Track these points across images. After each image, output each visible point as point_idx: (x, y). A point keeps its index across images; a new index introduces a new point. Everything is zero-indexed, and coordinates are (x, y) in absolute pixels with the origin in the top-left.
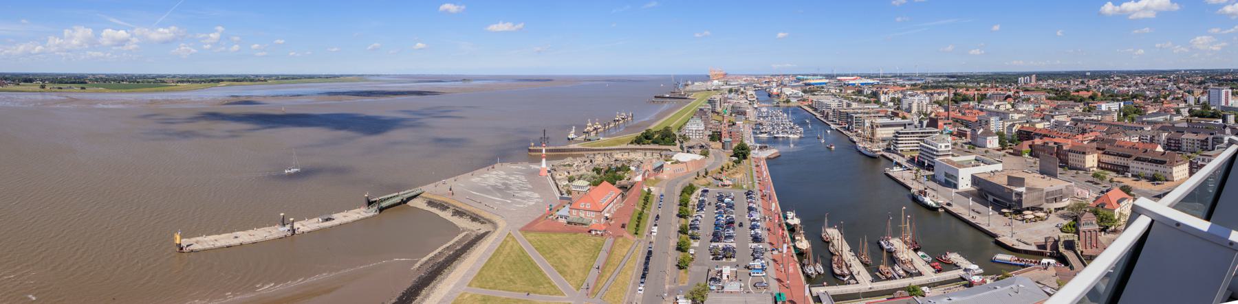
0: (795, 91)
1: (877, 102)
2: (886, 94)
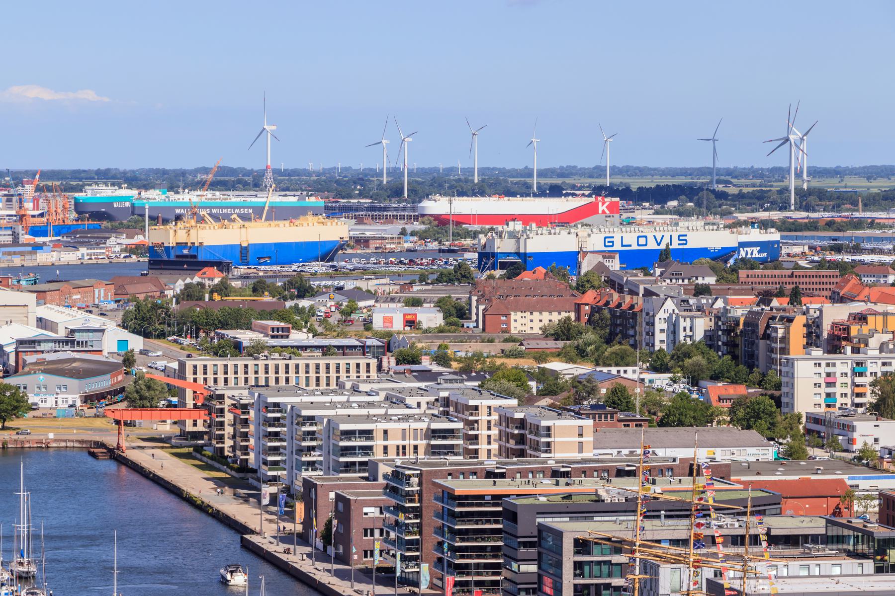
2: (834, 346)
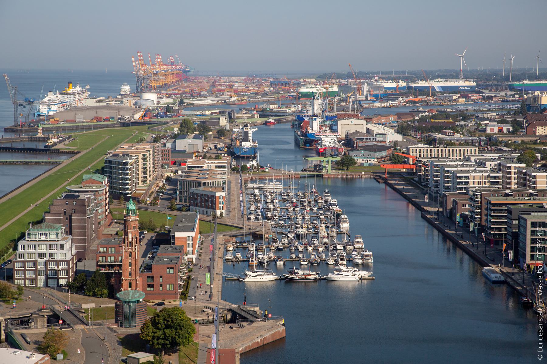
0: (376, 129)
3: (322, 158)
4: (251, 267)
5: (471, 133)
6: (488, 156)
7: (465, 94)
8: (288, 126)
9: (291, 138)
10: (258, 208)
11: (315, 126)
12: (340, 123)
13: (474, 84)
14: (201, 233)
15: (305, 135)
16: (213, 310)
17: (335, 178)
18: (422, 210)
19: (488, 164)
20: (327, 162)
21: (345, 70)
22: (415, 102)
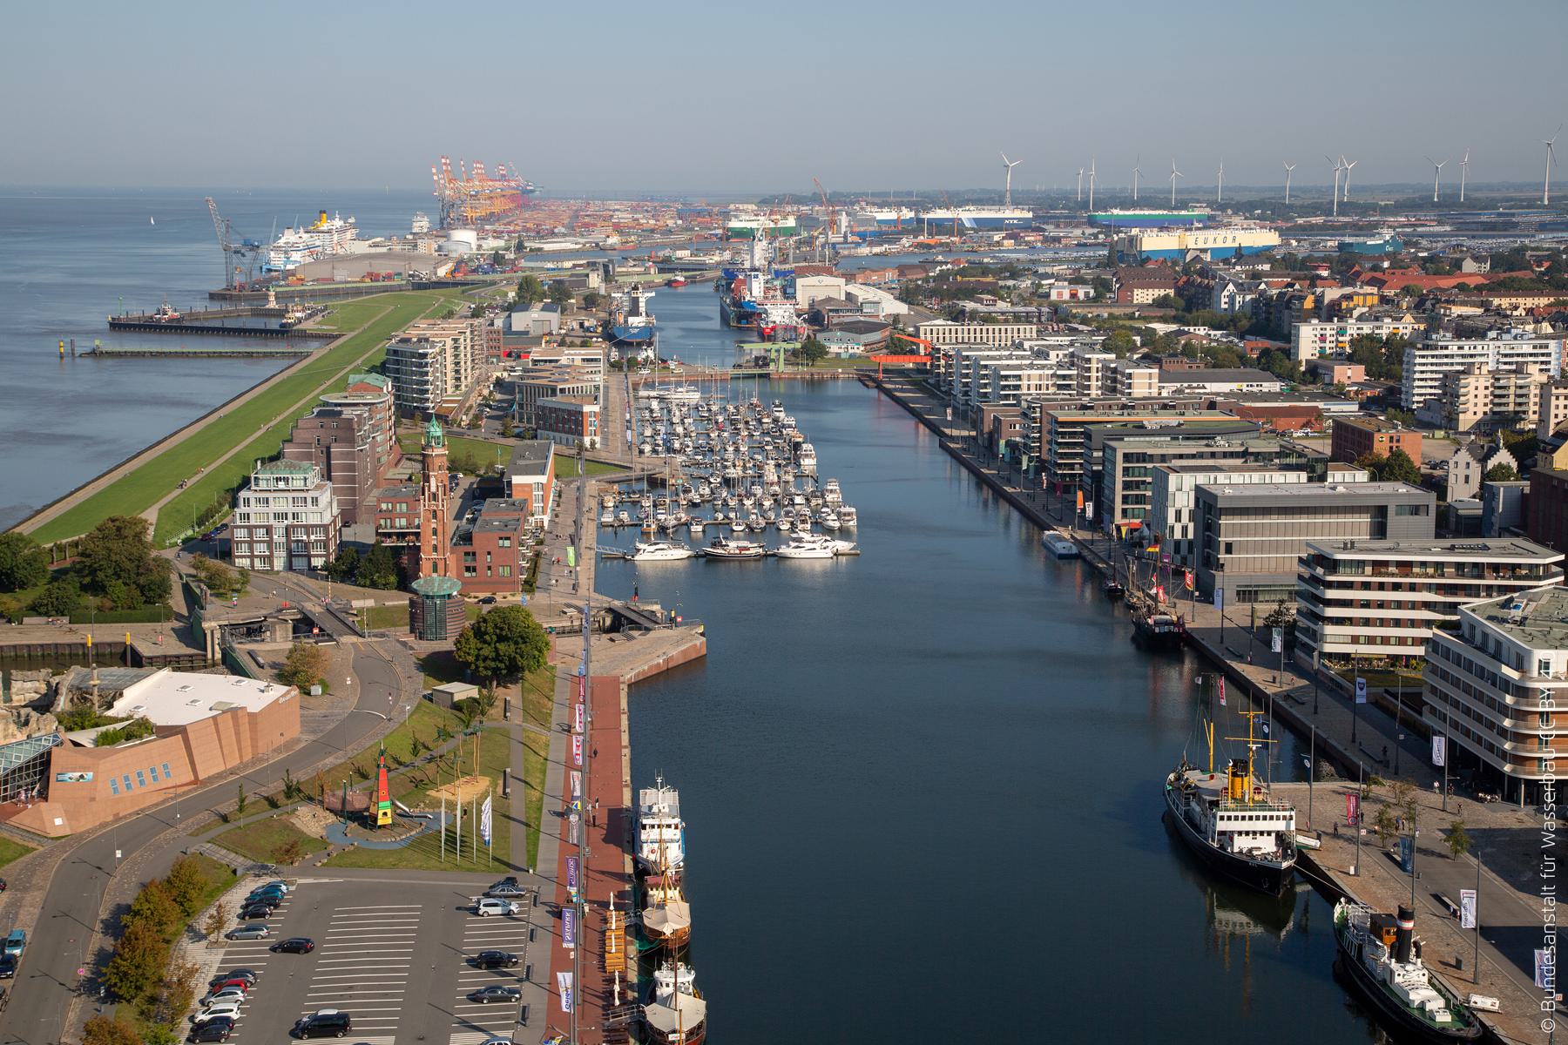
0: (862, 293)
1: (1281, 360)
3: (768, 345)
4: (645, 536)
5: (1024, 301)
6: (1052, 340)
7: (1015, 231)
8: (709, 288)
9: (714, 311)
10: (657, 433)
11: (756, 289)
12: (800, 282)
13: (1030, 215)
14: (557, 477)
15: (738, 303)
16: (580, 610)
17: (791, 380)
18: (942, 435)
19: (1053, 354)
20: (778, 351)
21: (806, 189)
22: (929, 247)
